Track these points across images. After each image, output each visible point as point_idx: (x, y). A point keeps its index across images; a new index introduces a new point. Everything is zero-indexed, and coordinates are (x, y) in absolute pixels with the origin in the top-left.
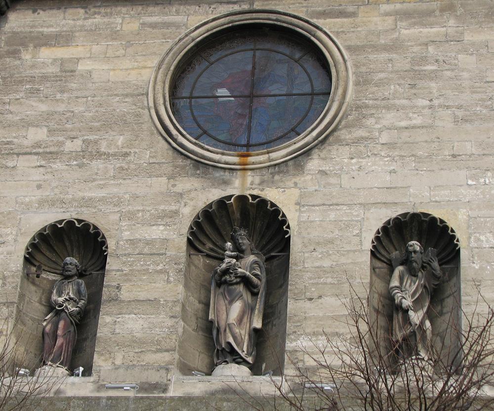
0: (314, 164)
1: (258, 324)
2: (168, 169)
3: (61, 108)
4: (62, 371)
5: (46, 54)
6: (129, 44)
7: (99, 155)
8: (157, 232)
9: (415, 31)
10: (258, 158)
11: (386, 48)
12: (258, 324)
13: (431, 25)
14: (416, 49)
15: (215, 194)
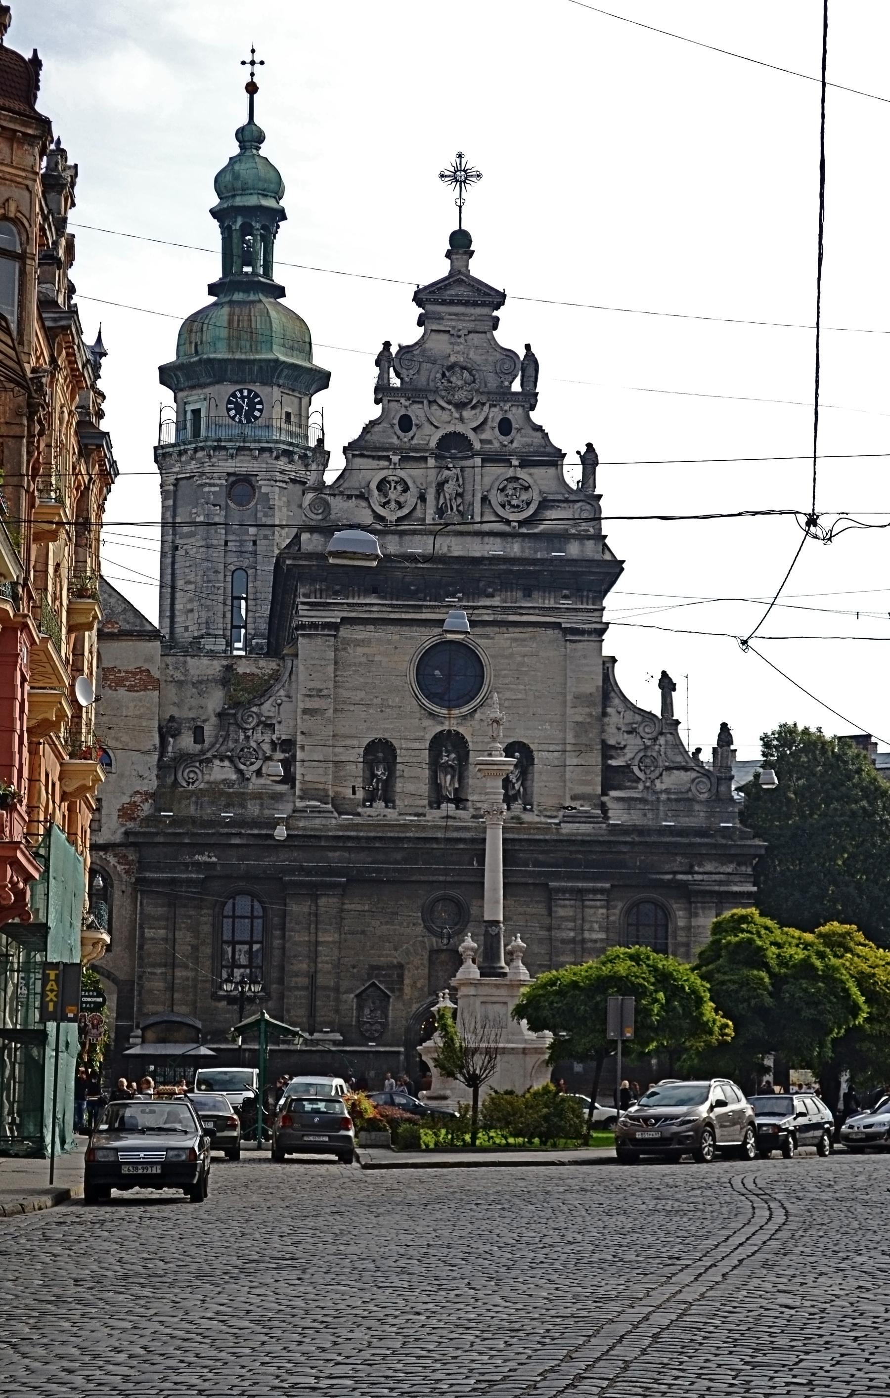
0: (477, 716)
1: (457, 786)
2: (418, 715)
3: (370, 681)
4: (383, 804)
5: (360, 650)
6: (396, 648)
7: (389, 706)
8: (416, 745)
9: (519, 649)
10: (456, 712)
11: (507, 657)
12: (457, 786)
13: (526, 646)
14: (519, 659)
15: (439, 729)
